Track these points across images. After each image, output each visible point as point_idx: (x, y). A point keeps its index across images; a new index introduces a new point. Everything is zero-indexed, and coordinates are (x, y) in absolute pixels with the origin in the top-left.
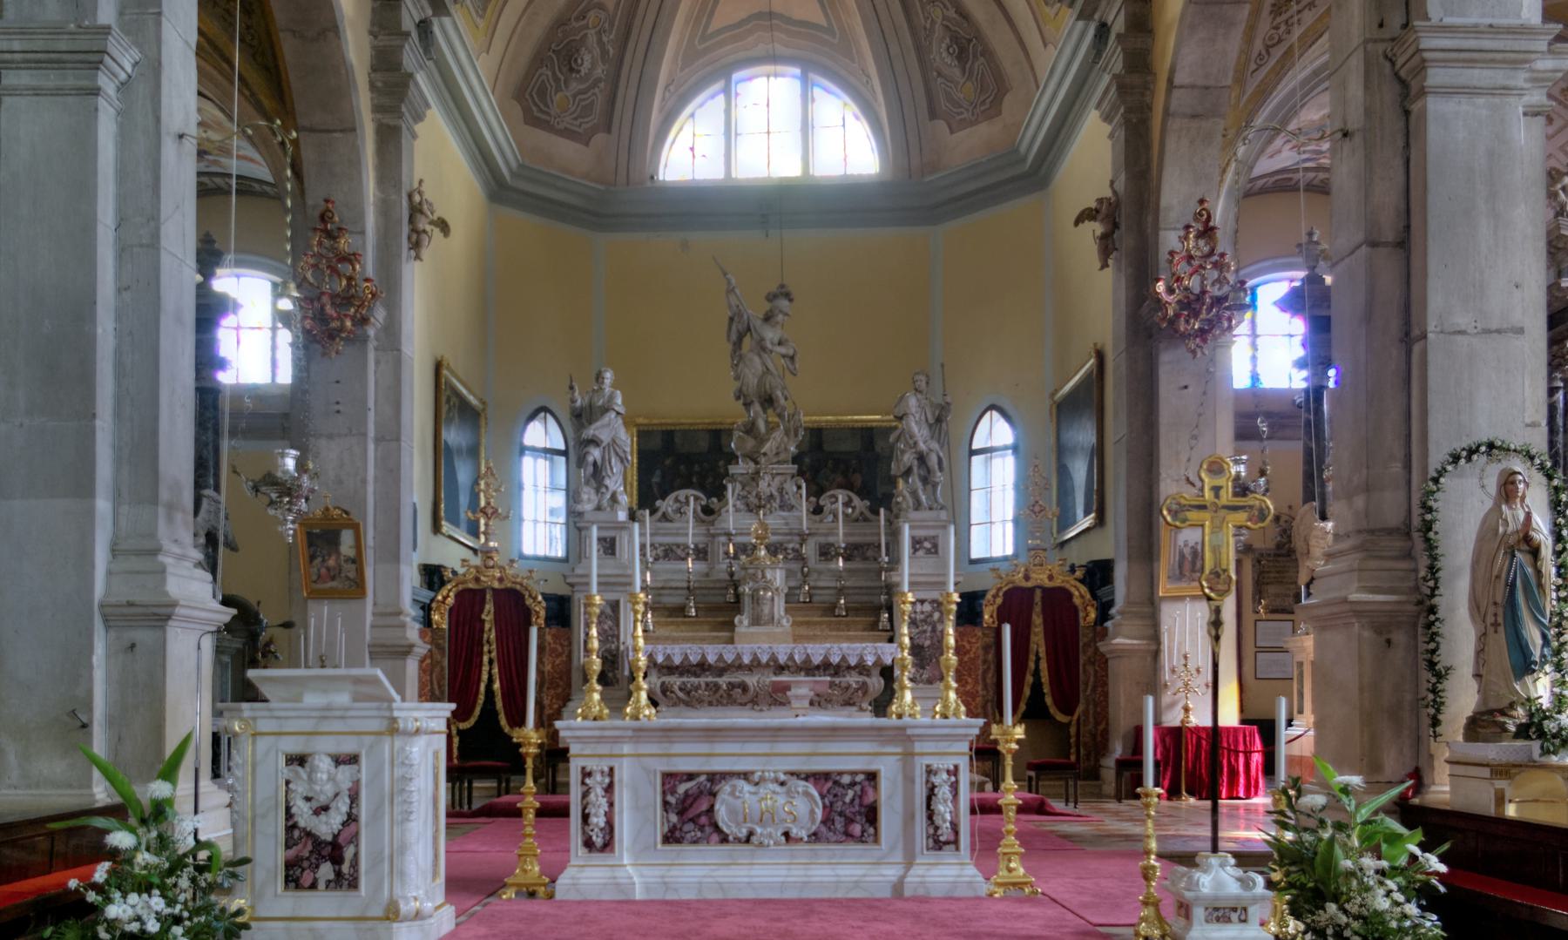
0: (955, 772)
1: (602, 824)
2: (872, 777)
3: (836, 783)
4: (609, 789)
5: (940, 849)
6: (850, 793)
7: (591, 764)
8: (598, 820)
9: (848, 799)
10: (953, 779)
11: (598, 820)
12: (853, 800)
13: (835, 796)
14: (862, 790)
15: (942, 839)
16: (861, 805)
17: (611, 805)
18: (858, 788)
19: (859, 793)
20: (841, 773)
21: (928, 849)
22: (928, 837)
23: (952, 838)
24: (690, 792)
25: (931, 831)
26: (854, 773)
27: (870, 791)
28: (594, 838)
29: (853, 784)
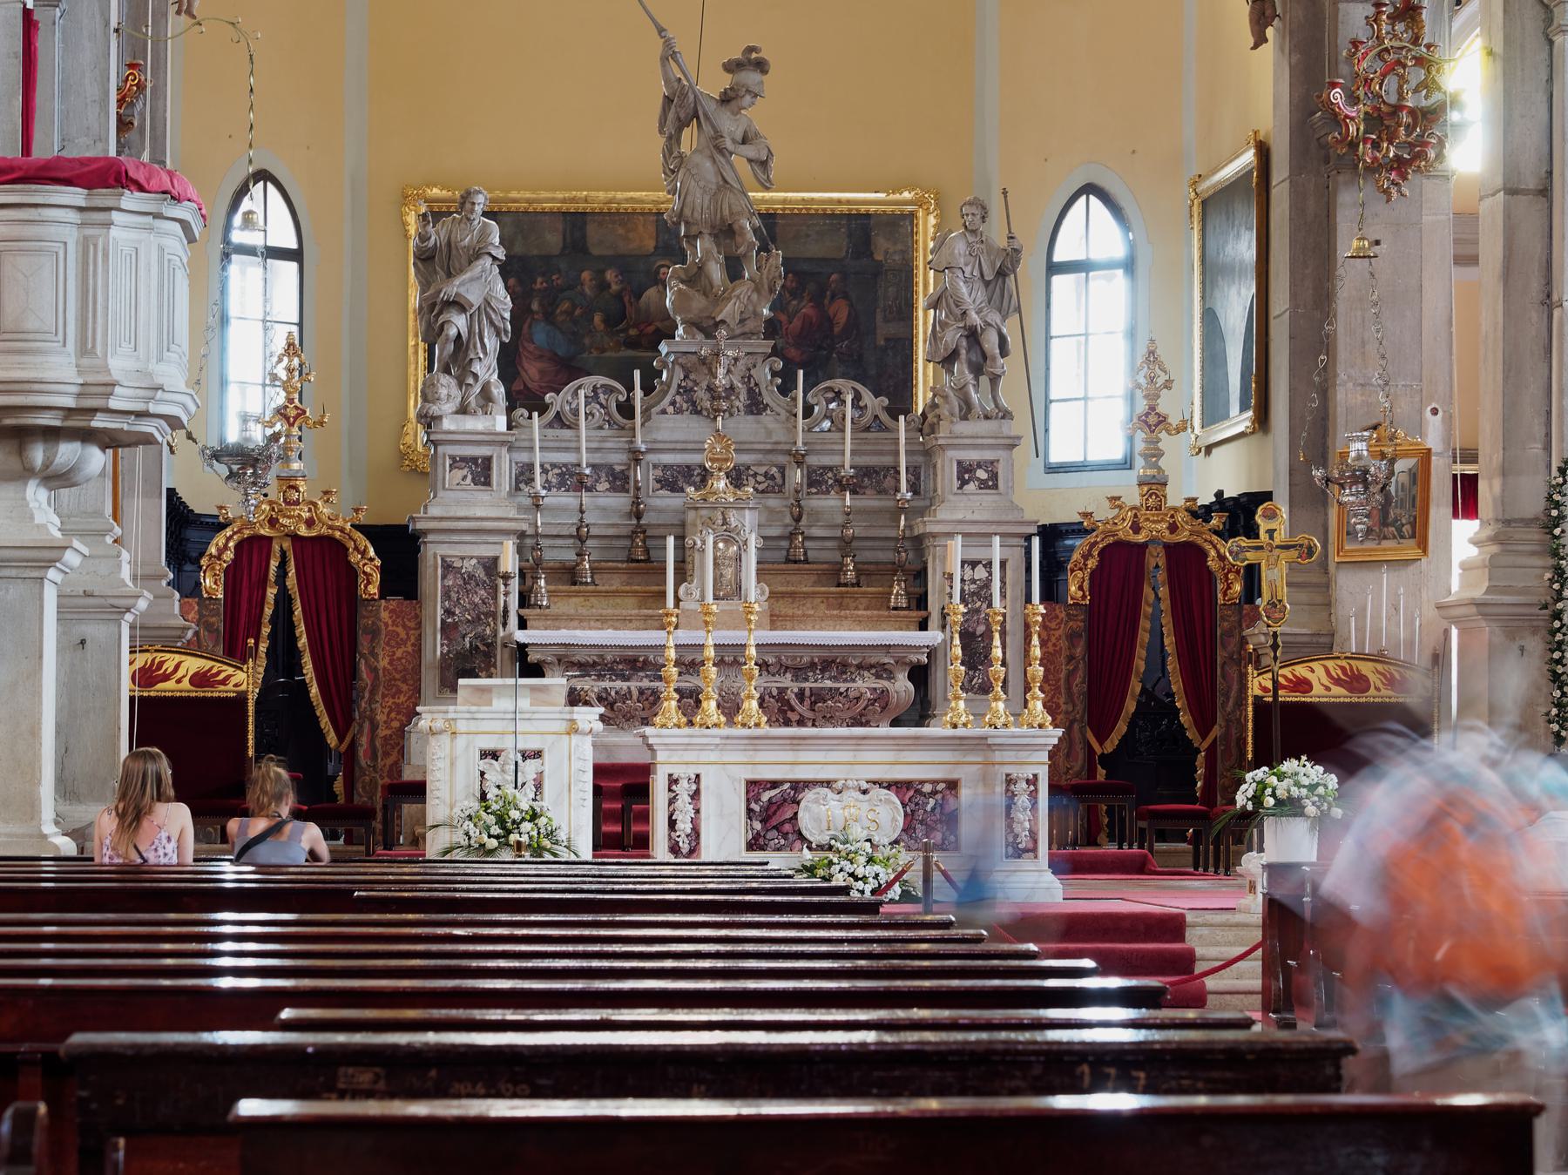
0: (1033, 781)
1: (689, 831)
2: (953, 785)
3: (918, 792)
4: (695, 796)
5: (1019, 857)
6: (932, 802)
7: (678, 771)
8: (684, 826)
9: (929, 808)
10: (1032, 788)
11: (684, 826)
12: (933, 809)
13: (917, 804)
14: (943, 798)
15: (1020, 846)
16: (941, 813)
17: (697, 811)
18: (939, 796)
19: (940, 802)
20: (922, 782)
21: (1007, 858)
22: (1007, 846)
23: (1031, 845)
24: (774, 800)
25: (1011, 839)
26: (935, 782)
27: (951, 800)
28: (681, 844)
29: (934, 793)
